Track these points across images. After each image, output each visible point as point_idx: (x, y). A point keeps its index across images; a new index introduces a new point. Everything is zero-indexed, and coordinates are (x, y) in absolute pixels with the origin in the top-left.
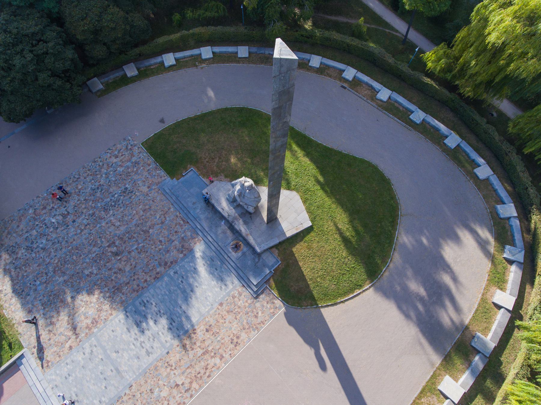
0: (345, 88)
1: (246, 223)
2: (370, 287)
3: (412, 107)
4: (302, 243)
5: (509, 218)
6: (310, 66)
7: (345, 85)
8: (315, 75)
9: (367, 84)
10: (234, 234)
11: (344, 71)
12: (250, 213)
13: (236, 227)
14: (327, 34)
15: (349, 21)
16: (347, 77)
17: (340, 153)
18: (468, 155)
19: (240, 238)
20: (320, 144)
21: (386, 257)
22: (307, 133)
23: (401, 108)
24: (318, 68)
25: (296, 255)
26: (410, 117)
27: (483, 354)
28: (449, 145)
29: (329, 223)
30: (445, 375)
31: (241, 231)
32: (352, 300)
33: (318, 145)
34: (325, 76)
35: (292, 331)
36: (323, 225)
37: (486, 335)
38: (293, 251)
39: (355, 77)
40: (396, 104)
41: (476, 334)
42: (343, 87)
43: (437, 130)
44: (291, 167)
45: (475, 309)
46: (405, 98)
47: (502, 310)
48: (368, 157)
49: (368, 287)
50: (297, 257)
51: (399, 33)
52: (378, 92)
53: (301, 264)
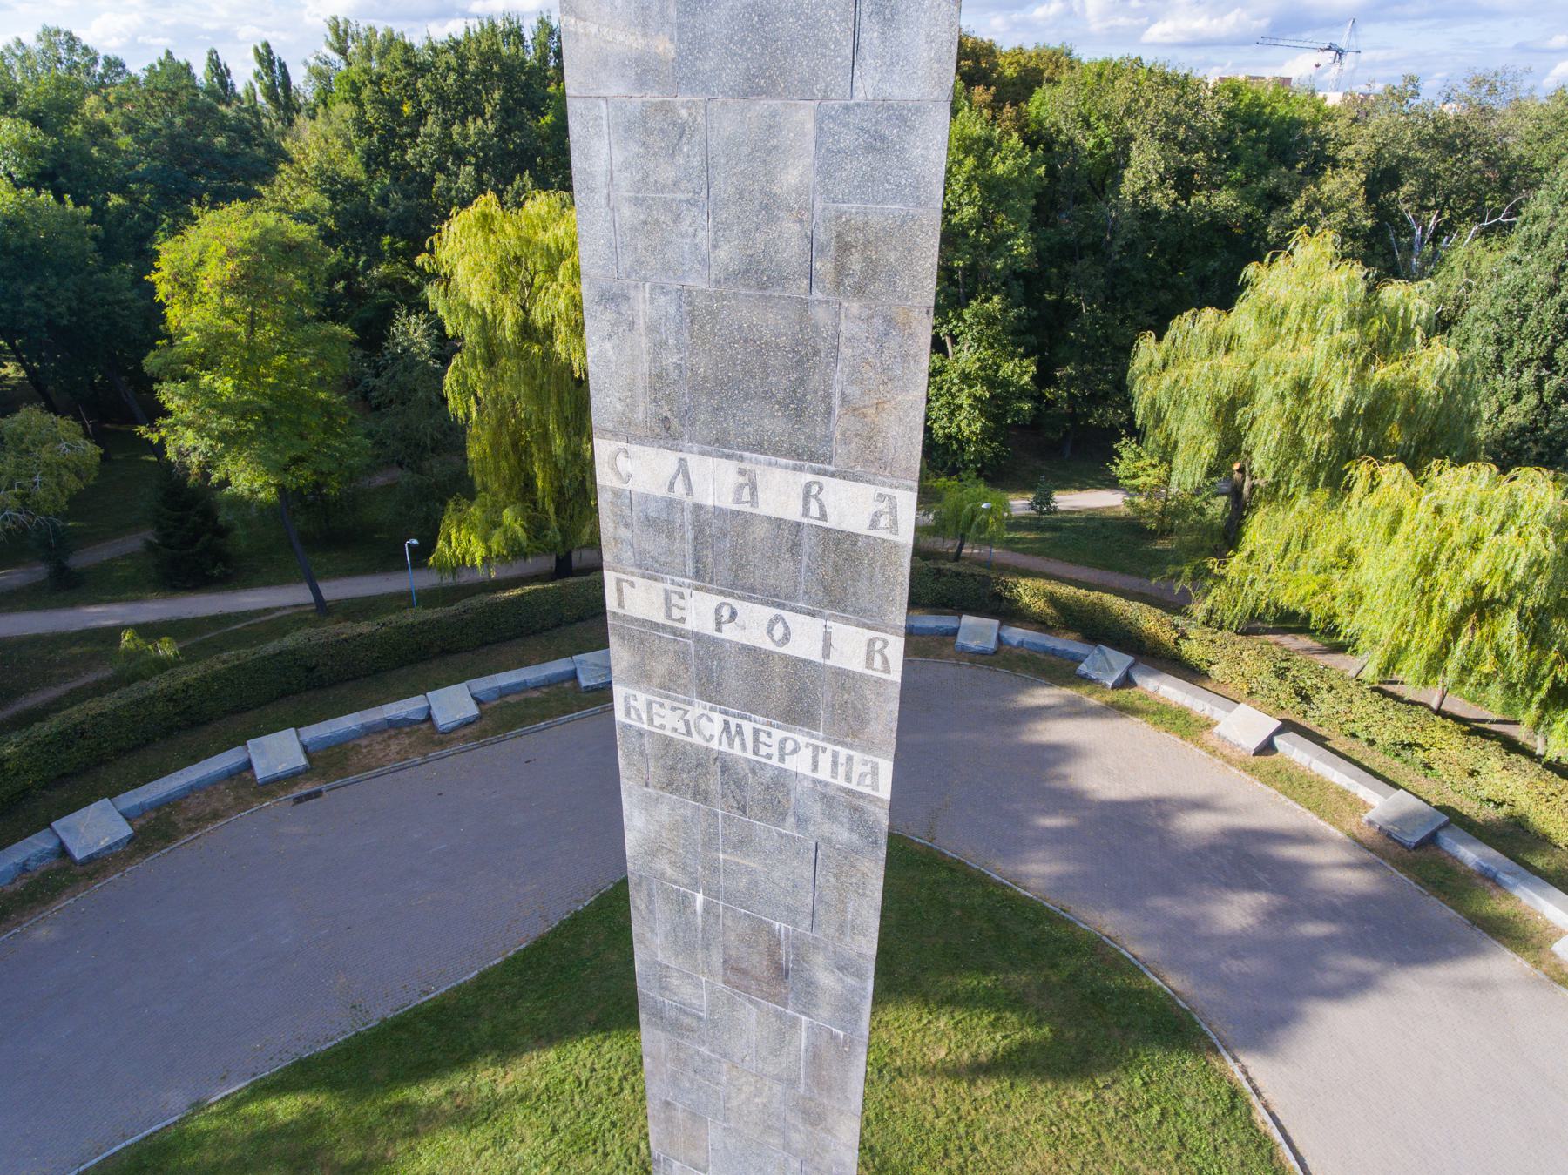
0: (318, 794)
2: (1236, 1060)
3: (559, 667)
5: (999, 638)
6: (91, 859)
7: (308, 788)
8: (143, 864)
9: (369, 730)
11: (248, 766)
14: (42, 730)
15: (72, 686)
16: (281, 768)
17: (576, 918)
20: (482, 976)
21: (1097, 948)
22: (383, 1010)
23: (536, 694)
24: (131, 839)
26: (584, 683)
27: (1441, 828)
29: (911, 1090)
30: (1554, 955)
32: (1308, 1161)
33: (483, 983)
34: (191, 831)
36: (918, 1124)
37: (1365, 806)
39: (305, 748)
40: (509, 699)
41: (1370, 823)
42: (299, 800)
44: (523, 1153)
45: (1283, 798)
46: (508, 669)
47: (1278, 741)
49: (1235, 1067)
51: (278, 609)
52: (429, 718)
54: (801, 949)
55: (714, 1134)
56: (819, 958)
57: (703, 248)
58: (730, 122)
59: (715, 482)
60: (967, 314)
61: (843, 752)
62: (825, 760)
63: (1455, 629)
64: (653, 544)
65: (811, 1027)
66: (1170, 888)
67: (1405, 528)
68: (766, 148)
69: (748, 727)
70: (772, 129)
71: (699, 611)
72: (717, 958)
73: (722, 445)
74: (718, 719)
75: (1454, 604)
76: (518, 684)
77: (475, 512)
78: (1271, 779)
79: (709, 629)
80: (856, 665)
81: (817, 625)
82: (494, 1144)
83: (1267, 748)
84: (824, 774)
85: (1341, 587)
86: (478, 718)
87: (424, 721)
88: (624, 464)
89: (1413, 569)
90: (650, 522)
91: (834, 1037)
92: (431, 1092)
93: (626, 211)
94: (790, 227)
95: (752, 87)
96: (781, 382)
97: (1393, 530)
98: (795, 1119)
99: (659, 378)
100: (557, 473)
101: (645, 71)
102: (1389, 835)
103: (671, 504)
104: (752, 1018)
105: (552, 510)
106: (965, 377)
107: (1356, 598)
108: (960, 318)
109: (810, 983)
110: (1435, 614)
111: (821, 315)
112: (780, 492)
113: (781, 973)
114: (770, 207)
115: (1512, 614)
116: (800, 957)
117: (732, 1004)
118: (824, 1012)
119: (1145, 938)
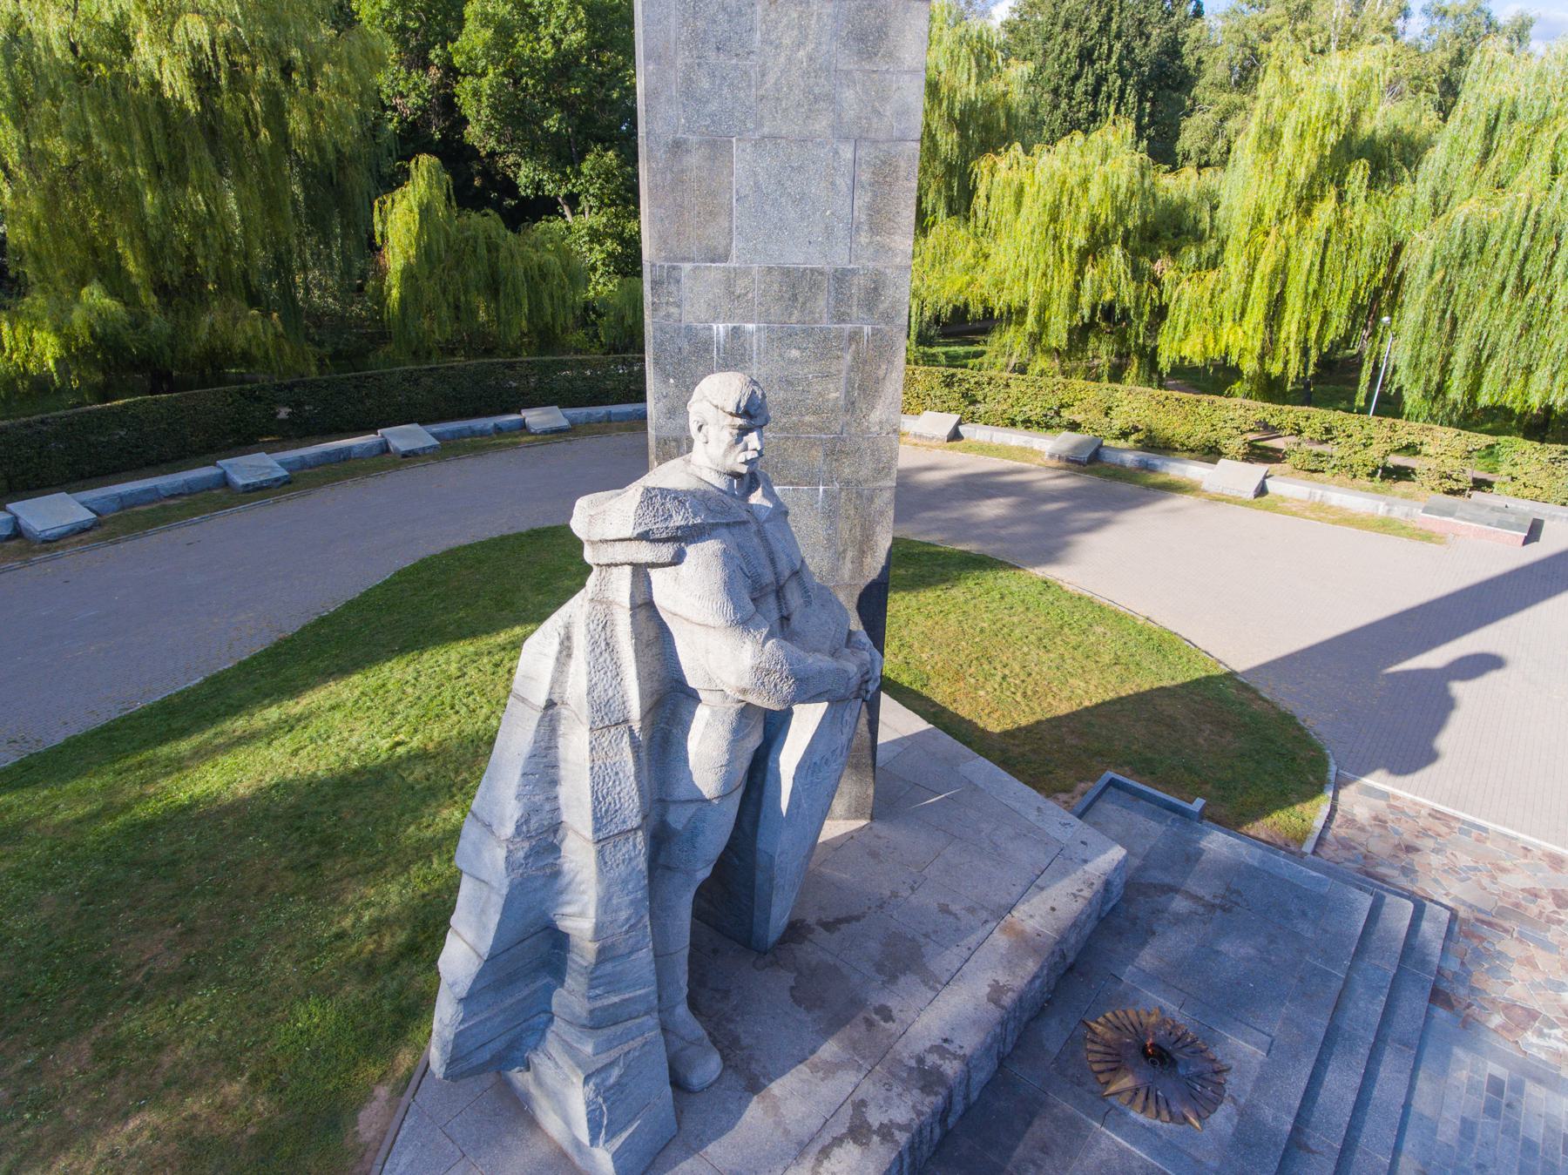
1: (905, 958)
4: (938, 699)
10: (1031, 1109)
12: (796, 931)
13: (969, 1042)
18: (473, 433)
19: (1053, 1035)
25: (1023, 722)
28: (421, 445)
31: (997, 991)
35: (1444, 742)
38: (1006, 734)
43: (344, 456)
47: (961, 428)
48: (404, 560)
50: (1032, 719)
53: (1063, 709)
55: (742, 162)
60: (585, 168)
63: (1080, 272)
66: (930, 508)
67: (1027, 201)
75: (1080, 240)
76: (147, 491)
77: (36, 301)
78: (969, 449)
82: (312, 740)
83: (955, 436)
85: (984, 279)
86: (95, 525)
87: (8, 538)
89: (1046, 218)
92: (184, 746)
97: (1019, 204)
98: (847, 62)
100: (153, 254)
102: (1068, 460)
105: (149, 299)
106: (595, 236)
107: (999, 285)
108: (578, 174)
110: (1066, 257)
115: (1117, 250)
119: (928, 532)
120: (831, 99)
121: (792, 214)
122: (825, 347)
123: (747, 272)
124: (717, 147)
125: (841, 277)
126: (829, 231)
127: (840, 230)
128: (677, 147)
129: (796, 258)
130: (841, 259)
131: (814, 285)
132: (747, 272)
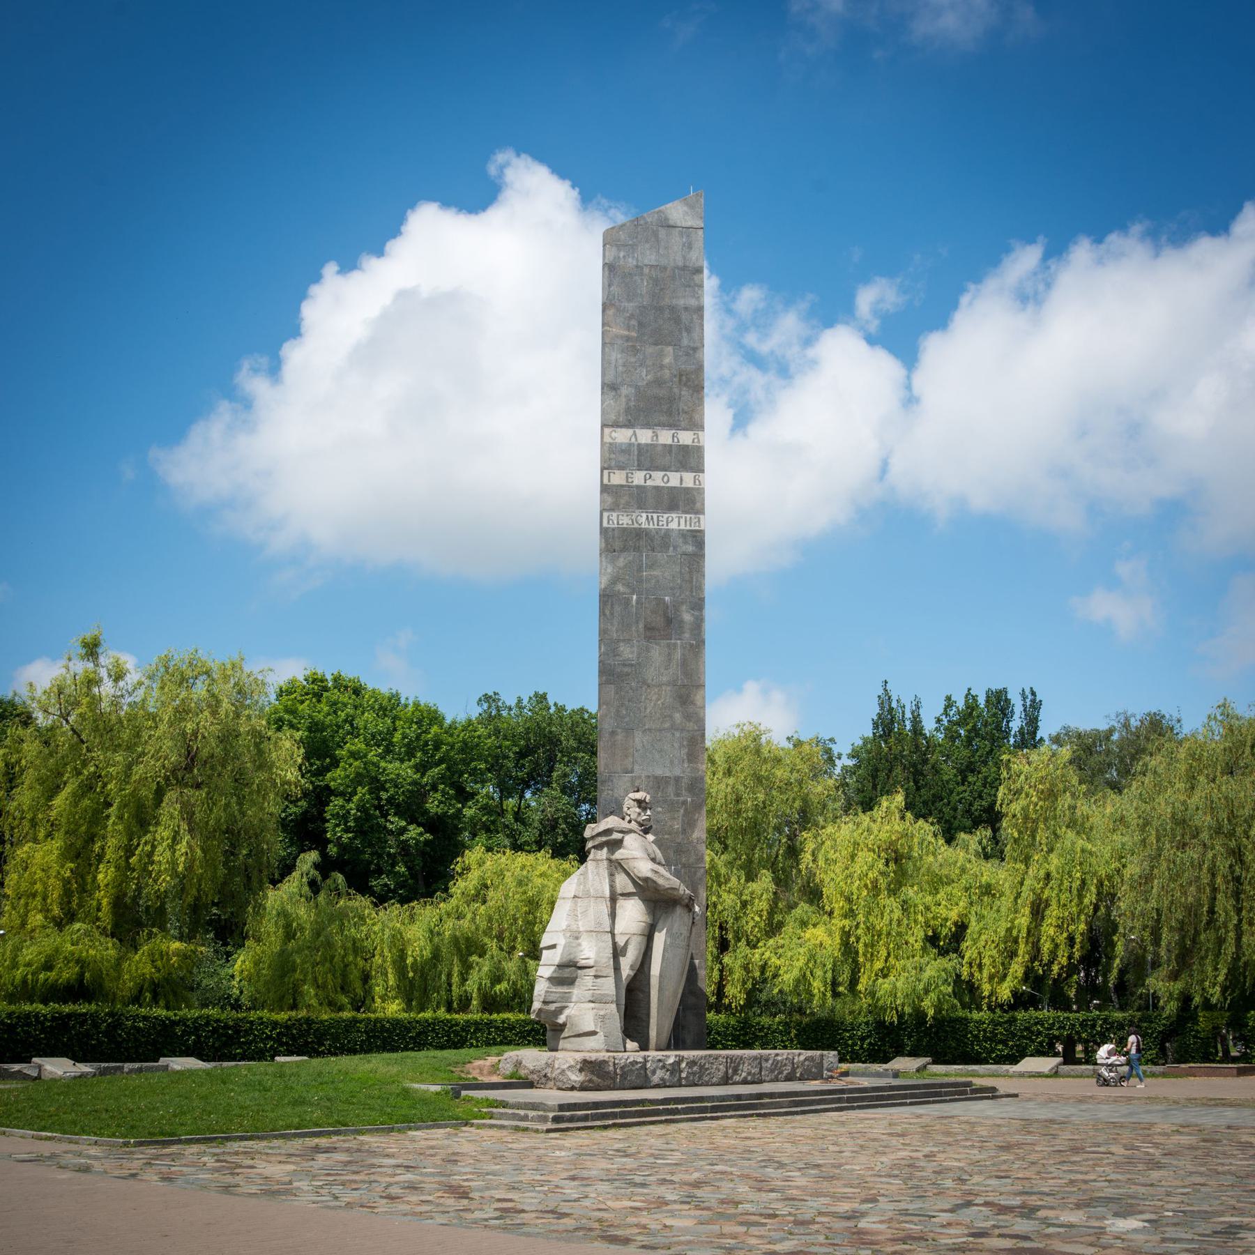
54: (677, 606)
56: (684, 608)
57: (644, 376)
58: (650, 350)
59: (644, 436)
61: (688, 516)
62: (682, 521)
64: (622, 458)
65: (683, 648)
68: (661, 355)
69: (655, 516)
70: (662, 351)
71: (638, 478)
72: (641, 626)
73: (647, 425)
74: (644, 515)
79: (642, 483)
80: (691, 485)
81: (678, 475)
84: (682, 527)
88: (614, 434)
90: (622, 451)
91: (691, 645)
93: (621, 368)
94: (667, 371)
95: (656, 344)
96: (665, 407)
99: (628, 410)
101: (628, 339)
103: (630, 445)
104: (657, 653)
109: (681, 621)
111: (676, 390)
112: (665, 437)
113: (669, 621)
114: (662, 367)
116: (677, 610)
117: (648, 650)
118: (687, 635)
120: (671, 717)
121: (657, 756)
122: (672, 807)
123: (640, 777)
124: (629, 731)
125: (677, 779)
126: (672, 762)
127: (676, 762)
128: (613, 733)
129: (659, 772)
130: (677, 772)
131: (667, 783)
132: (640, 777)
